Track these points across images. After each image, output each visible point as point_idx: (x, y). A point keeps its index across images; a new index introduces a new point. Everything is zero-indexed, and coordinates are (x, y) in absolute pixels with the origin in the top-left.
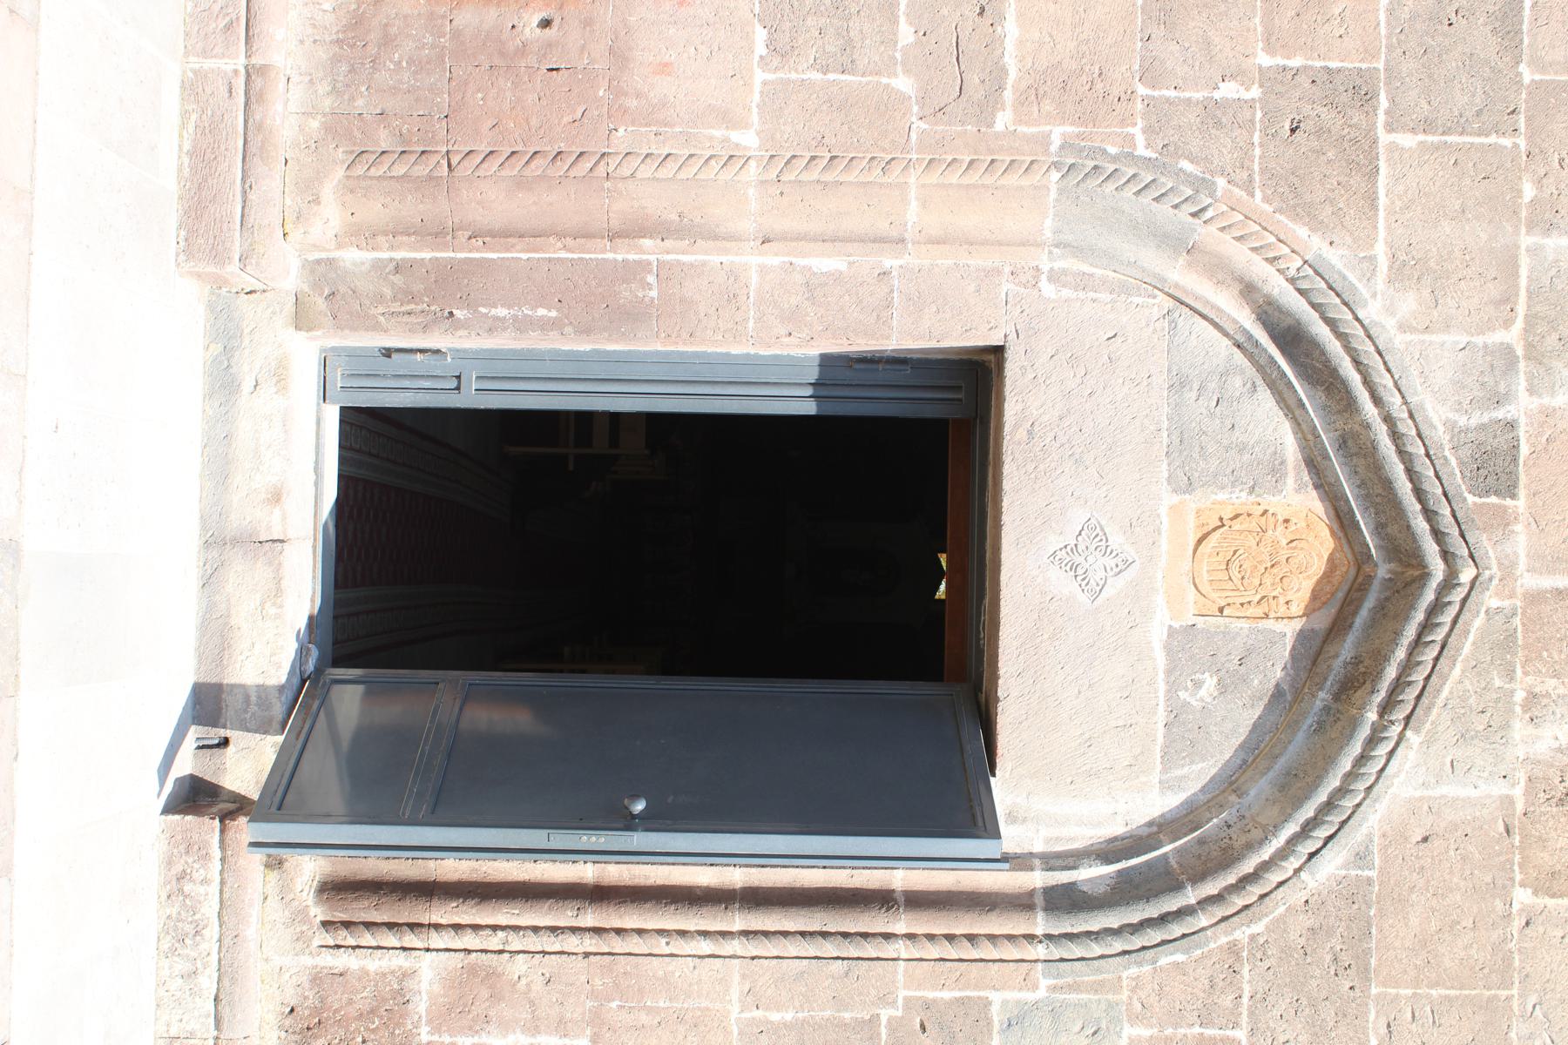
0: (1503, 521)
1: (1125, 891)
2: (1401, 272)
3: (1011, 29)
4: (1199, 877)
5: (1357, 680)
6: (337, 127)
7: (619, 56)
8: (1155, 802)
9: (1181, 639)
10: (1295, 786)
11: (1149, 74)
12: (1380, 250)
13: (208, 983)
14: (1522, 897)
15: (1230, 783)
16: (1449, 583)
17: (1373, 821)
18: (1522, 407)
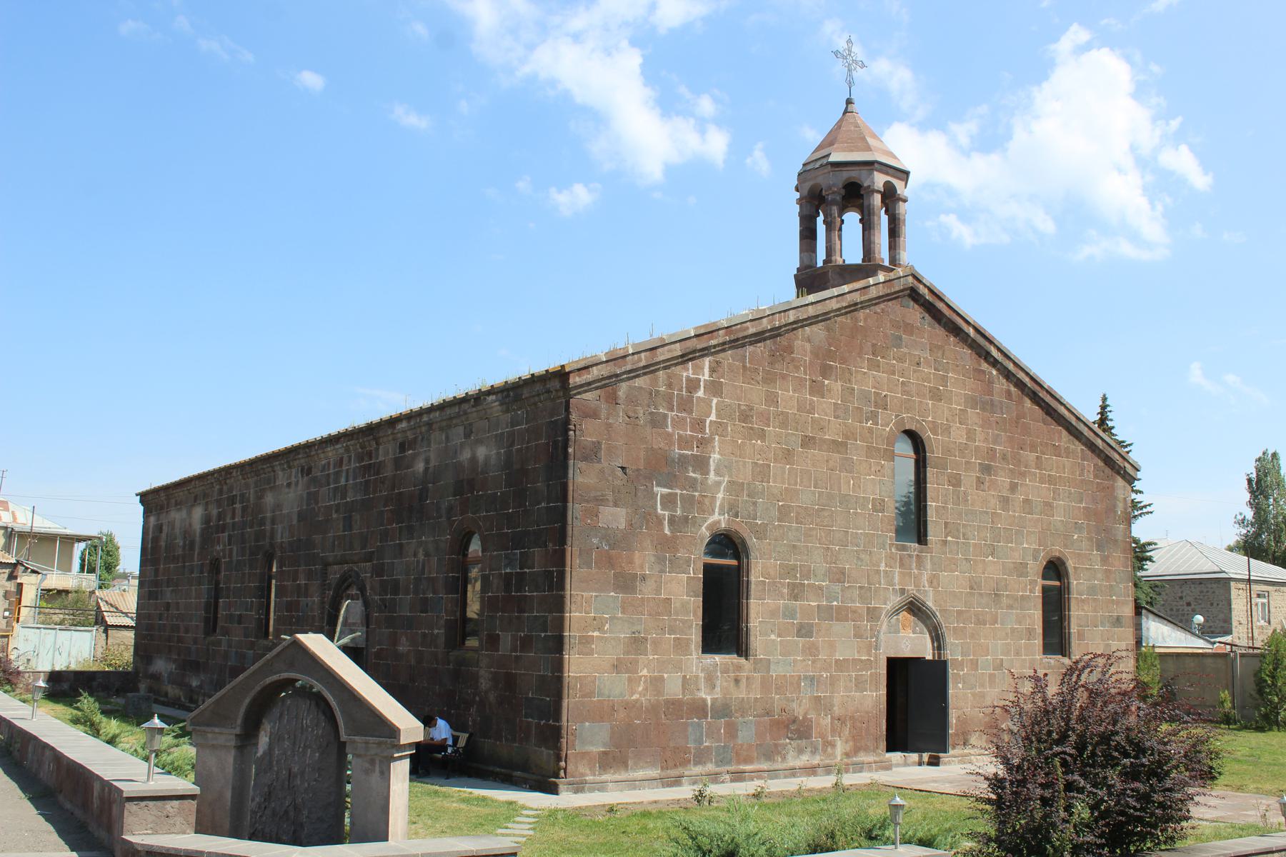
0: (908, 590)
1: (938, 640)
2: (885, 604)
3: (863, 658)
4: (938, 631)
5: (919, 609)
6: (874, 751)
7: (867, 713)
8: (928, 636)
9: (914, 632)
10: (929, 617)
11: (867, 639)
12: (883, 606)
13: (953, 759)
14: (940, 589)
15: (926, 626)
16: (913, 598)
17: (934, 608)
18: (897, 587)
